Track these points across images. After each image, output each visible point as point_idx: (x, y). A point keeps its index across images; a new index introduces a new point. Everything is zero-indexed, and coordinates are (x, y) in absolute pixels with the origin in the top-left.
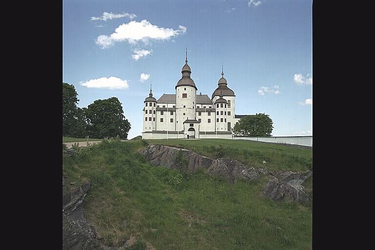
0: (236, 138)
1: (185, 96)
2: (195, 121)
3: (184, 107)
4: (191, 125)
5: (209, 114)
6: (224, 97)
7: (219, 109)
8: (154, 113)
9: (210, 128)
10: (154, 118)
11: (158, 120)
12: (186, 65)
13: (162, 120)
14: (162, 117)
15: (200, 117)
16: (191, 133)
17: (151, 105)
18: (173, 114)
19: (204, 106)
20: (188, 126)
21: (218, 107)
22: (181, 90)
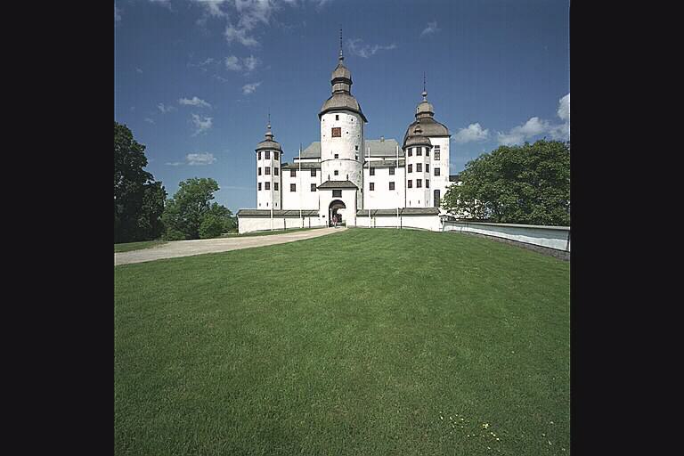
0: (449, 228)
1: (336, 132)
2: (349, 185)
3: (336, 156)
4: (337, 193)
5: (392, 173)
9: (394, 201)
10: (276, 184)
11: (286, 187)
13: (293, 188)
14: (293, 180)
17: (267, 157)
20: (327, 196)
21: (410, 154)
22: (329, 121)
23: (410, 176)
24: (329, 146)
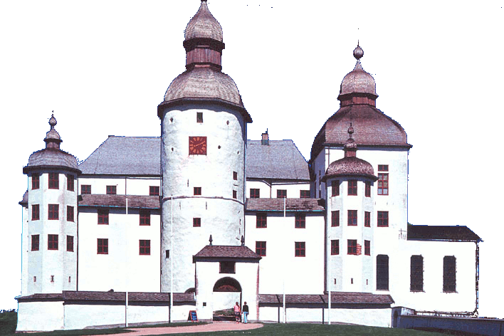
3: (198, 191)
4: (228, 265)
5: (300, 224)
6: (361, 154)
8: (70, 218)
10: (70, 239)
11: (87, 245)
13: (103, 246)
14: (103, 231)
15: (261, 234)
16: (226, 301)
18: (148, 223)
19: (276, 188)
21: (336, 193)
23: (333, 233)
24: (185, 171)
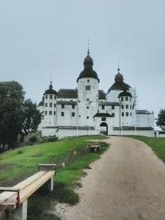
4: (104, 119)
7: (125, 103)
11: (59, 114)
12: (88, 56)
17: (51, 98)
21: (122, 100)
